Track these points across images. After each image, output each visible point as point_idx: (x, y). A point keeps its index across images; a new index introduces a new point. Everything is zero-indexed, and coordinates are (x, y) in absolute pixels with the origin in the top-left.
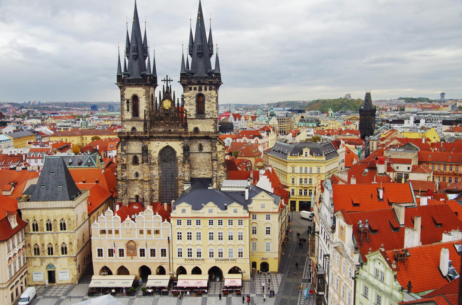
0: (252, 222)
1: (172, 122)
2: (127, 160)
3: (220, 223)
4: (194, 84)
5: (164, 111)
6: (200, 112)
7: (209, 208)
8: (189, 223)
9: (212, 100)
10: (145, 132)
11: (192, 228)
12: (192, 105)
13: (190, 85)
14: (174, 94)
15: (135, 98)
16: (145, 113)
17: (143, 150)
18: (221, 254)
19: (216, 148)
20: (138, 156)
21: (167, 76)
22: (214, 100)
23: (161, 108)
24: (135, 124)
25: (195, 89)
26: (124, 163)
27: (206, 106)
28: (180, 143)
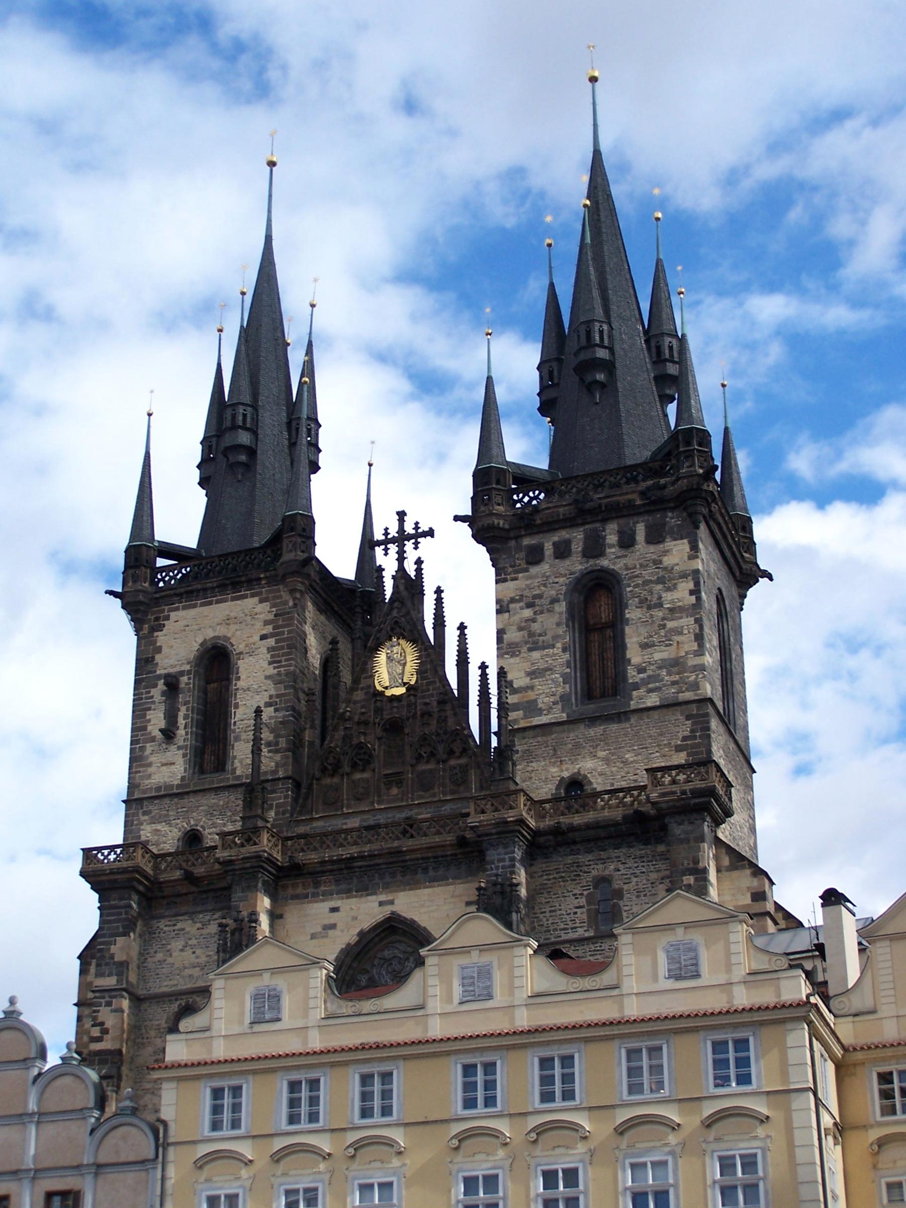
0: (874, 1134)
1: (422, 767)
3: (556, 1082)
4: (550, 526)
5: (378, 711)
6: (601, 686)
7: (456, 963)
8: (303, 1101)
9: (668, 596)
10: (249, 834)
11: (324, 1143)
12: (544, 648)
14: (439, 602)
16: (257, 729)
19: (701, 874)
21: (401, 515)
22: (682, 593)
23: (359, 695)
25: (562, 551)
27: (633, 638)
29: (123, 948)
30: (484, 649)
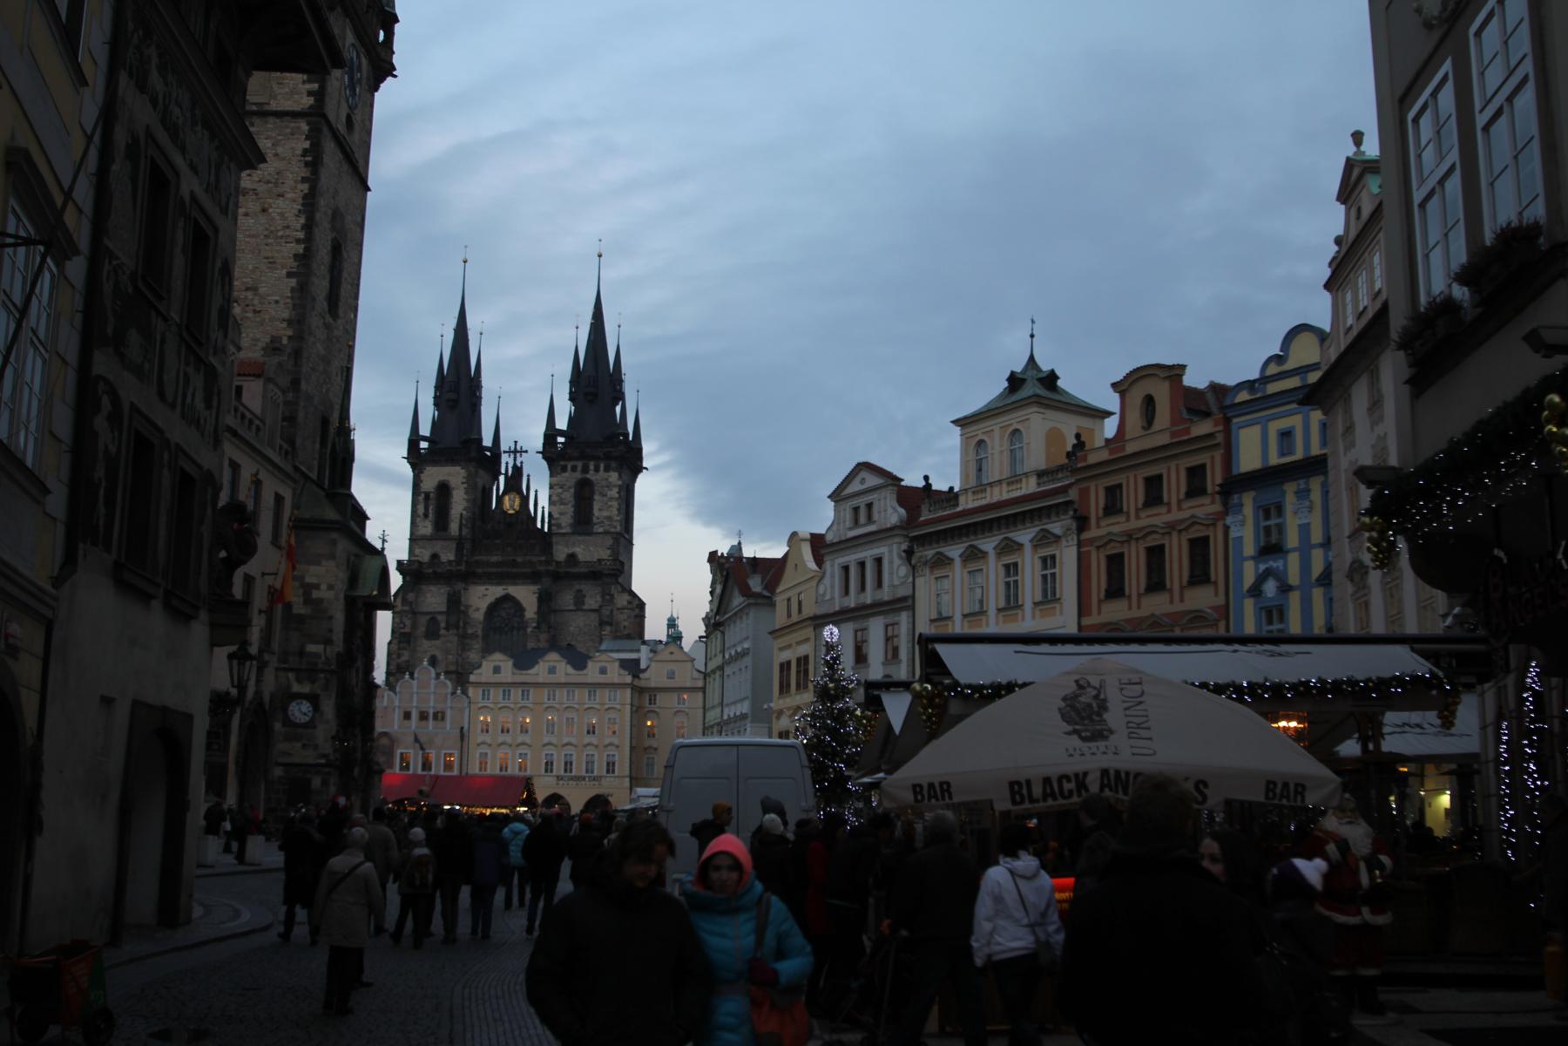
2: (414, 626)
4: (571, 459)
8: (507, 695)
10: (458, 562)
13: (564, 459)
15: (444, 489)
17: (449, 601)
18: (568, 765)
19: (612, 596)
20: (440, 618)
22: (614, 493)
24: (438, 547)
25: (574, 469)
26: (407, 630)
27: (596, 507)
28: (535, 588)
29: (411, 596)
30: (544, 502)
